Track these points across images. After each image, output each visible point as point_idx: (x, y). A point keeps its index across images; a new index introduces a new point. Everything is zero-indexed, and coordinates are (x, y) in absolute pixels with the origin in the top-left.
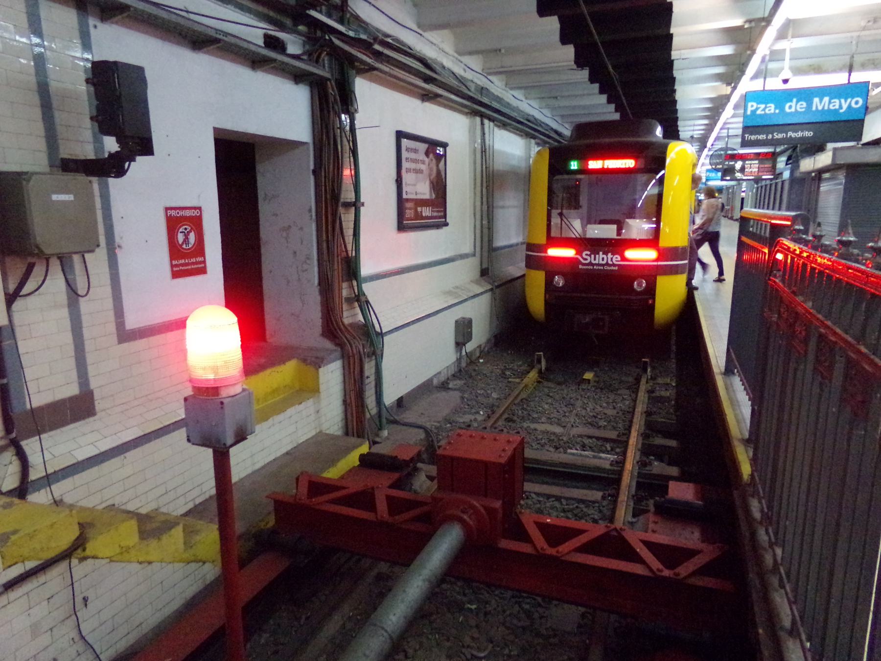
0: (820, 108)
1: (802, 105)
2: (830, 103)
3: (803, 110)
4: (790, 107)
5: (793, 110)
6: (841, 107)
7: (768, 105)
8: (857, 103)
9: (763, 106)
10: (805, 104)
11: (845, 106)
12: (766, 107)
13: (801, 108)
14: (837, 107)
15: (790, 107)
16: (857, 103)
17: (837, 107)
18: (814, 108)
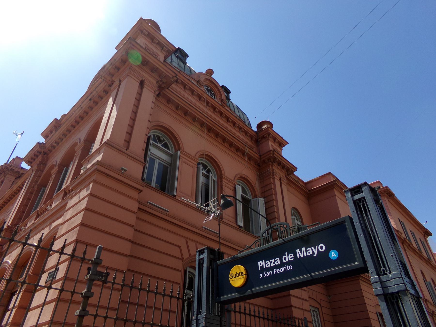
0: (302, 256)
1: (291, 256)
2: (306, 251)
3: (293, 259)
4: (285, 259)
5: (287, 260)
6: (314, 253)
7: (276, 259)
8: (322, 248)
9: (273, 260)
10: (293, 256)
11: (316, 252)
12: (275, 261)
13: (291, 258)
14: (311, 253)
15: (285, 259)
16: (322, 248)
17: (311, 253)
18: (298, 257)
